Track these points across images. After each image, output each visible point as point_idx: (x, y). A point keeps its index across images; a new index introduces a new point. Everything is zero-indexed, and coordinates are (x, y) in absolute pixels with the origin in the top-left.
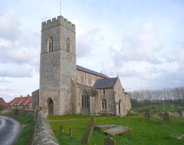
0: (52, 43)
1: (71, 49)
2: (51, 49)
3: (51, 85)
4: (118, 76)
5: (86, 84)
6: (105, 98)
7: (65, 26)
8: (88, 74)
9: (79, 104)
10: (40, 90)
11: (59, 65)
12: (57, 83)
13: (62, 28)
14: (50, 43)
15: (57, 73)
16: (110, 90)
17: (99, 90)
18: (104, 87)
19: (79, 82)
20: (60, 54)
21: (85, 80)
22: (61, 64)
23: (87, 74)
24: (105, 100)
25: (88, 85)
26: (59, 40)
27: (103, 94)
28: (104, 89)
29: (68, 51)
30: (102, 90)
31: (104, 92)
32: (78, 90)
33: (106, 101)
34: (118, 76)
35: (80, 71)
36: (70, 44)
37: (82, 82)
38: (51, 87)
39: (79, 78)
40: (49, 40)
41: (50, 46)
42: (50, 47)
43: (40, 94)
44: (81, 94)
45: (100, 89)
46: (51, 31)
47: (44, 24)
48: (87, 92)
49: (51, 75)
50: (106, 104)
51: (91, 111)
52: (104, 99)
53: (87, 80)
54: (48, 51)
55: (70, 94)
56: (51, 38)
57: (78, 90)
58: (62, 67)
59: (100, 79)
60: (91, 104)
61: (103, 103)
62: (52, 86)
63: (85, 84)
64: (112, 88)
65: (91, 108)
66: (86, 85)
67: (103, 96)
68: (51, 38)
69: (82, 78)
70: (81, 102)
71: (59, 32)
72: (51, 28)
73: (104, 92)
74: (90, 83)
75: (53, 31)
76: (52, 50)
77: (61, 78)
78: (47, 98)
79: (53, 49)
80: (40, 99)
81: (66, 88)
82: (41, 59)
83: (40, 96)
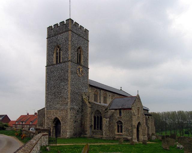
0: (60, 53)
1: (82, 61)
3: (58, 103)
4: (138, 95)
5: (100, 103)
6: (121, 120)
7: (75, 32)
8: (104, 91)
9: (91, 126)
10: (46, 109)
14: (57, 53)
15: (66, 89)
21: (99, 98)
23: (101, 91)
24: (121, 122)
25: (102, 104)
27: (118, 116)
29: (79, 63)
30: (118, 111)
31: (120, 113)
32: (89, 110)
33: (122, 124)
34: (138, 95)
35: (93, 88)
36: (81, 55)
37: (95, 101)
38: (58, 106)
39: (92, 96)
40: (55, 49)
41: (57, 57)
44: (93, 115)
46: (59, 38)
47: (50, 28)
48: (100, 113)
49: (58, 92)
50: (121, 127)
51: (104, 134)
52: (120, 121)
53: (102, 98)
54: (55, 62)
60: (104, 126)
61: (118, 126)
62: (59, 105)
65: (104, 131)
66: (100, 104)
67: (119, 117)
68: (59, 47)
69: (96, 96)
70: (93, 124)
72: (58, 34)
73: (120, 113)
74: (105, 102)
75: (61, 38)
76: (60, 63)
78: (53, 117)
79: (61, 61)
81: (75, 107)
82: (47, 73)
83: (46, 115)
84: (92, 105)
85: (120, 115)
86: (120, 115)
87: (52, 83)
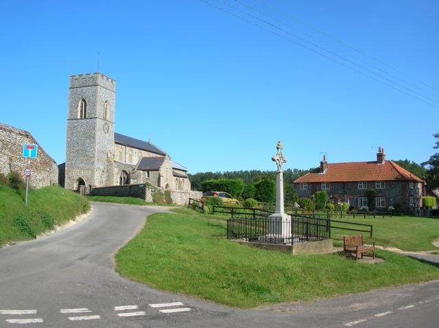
2: (84, 115)
11: (94, 138)
12: (90, 161)
13: (99, 89)
16: (156, 172)
17: (141, 171)
18: (148, 168)
19: (117, 160)
20: (95, 123)
22: (97, 137)
25: (128, 162)
26: (94, 105)
28: (148, 171)
31: (148, 174)
32: (116, 170)
38: (82, 165)
39: (117, 154)
42: (81, 112)
43: (66, 172)
44: (119, 176)
45: (143, 170)
53: (127, 156)
54: (79, 117)
55: (106, 175)
56: (84, 100)
57: (116, 170)
58: (97, 141)
59: (148, 156)
63: (124, 162)
64: (158, 170)
68: (84, 100)
71: (95, 94)
73: (148, 174)
74: (131, 159)
75: (87, 91)
77: (96, 155)
78: (77, 178)
80: (66, 178)
83: (66, 175)
84: (119, 164)
85: (148, 176)
86: (148, 176)
87: (75, 139)
